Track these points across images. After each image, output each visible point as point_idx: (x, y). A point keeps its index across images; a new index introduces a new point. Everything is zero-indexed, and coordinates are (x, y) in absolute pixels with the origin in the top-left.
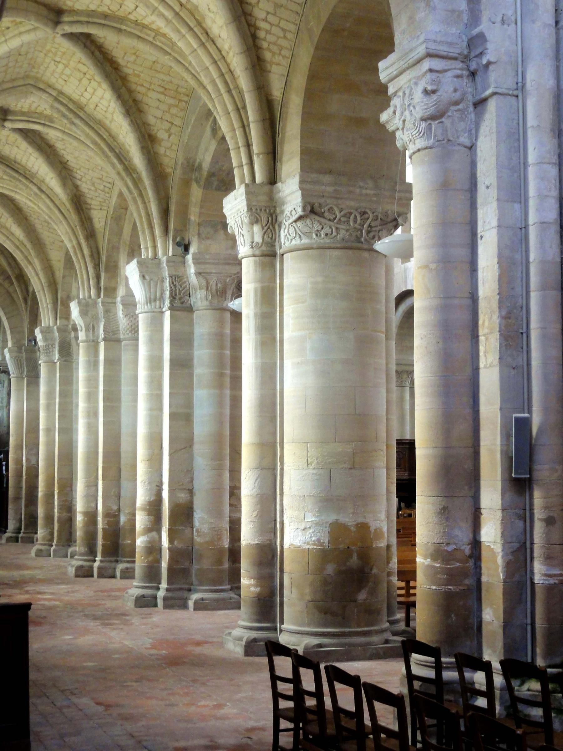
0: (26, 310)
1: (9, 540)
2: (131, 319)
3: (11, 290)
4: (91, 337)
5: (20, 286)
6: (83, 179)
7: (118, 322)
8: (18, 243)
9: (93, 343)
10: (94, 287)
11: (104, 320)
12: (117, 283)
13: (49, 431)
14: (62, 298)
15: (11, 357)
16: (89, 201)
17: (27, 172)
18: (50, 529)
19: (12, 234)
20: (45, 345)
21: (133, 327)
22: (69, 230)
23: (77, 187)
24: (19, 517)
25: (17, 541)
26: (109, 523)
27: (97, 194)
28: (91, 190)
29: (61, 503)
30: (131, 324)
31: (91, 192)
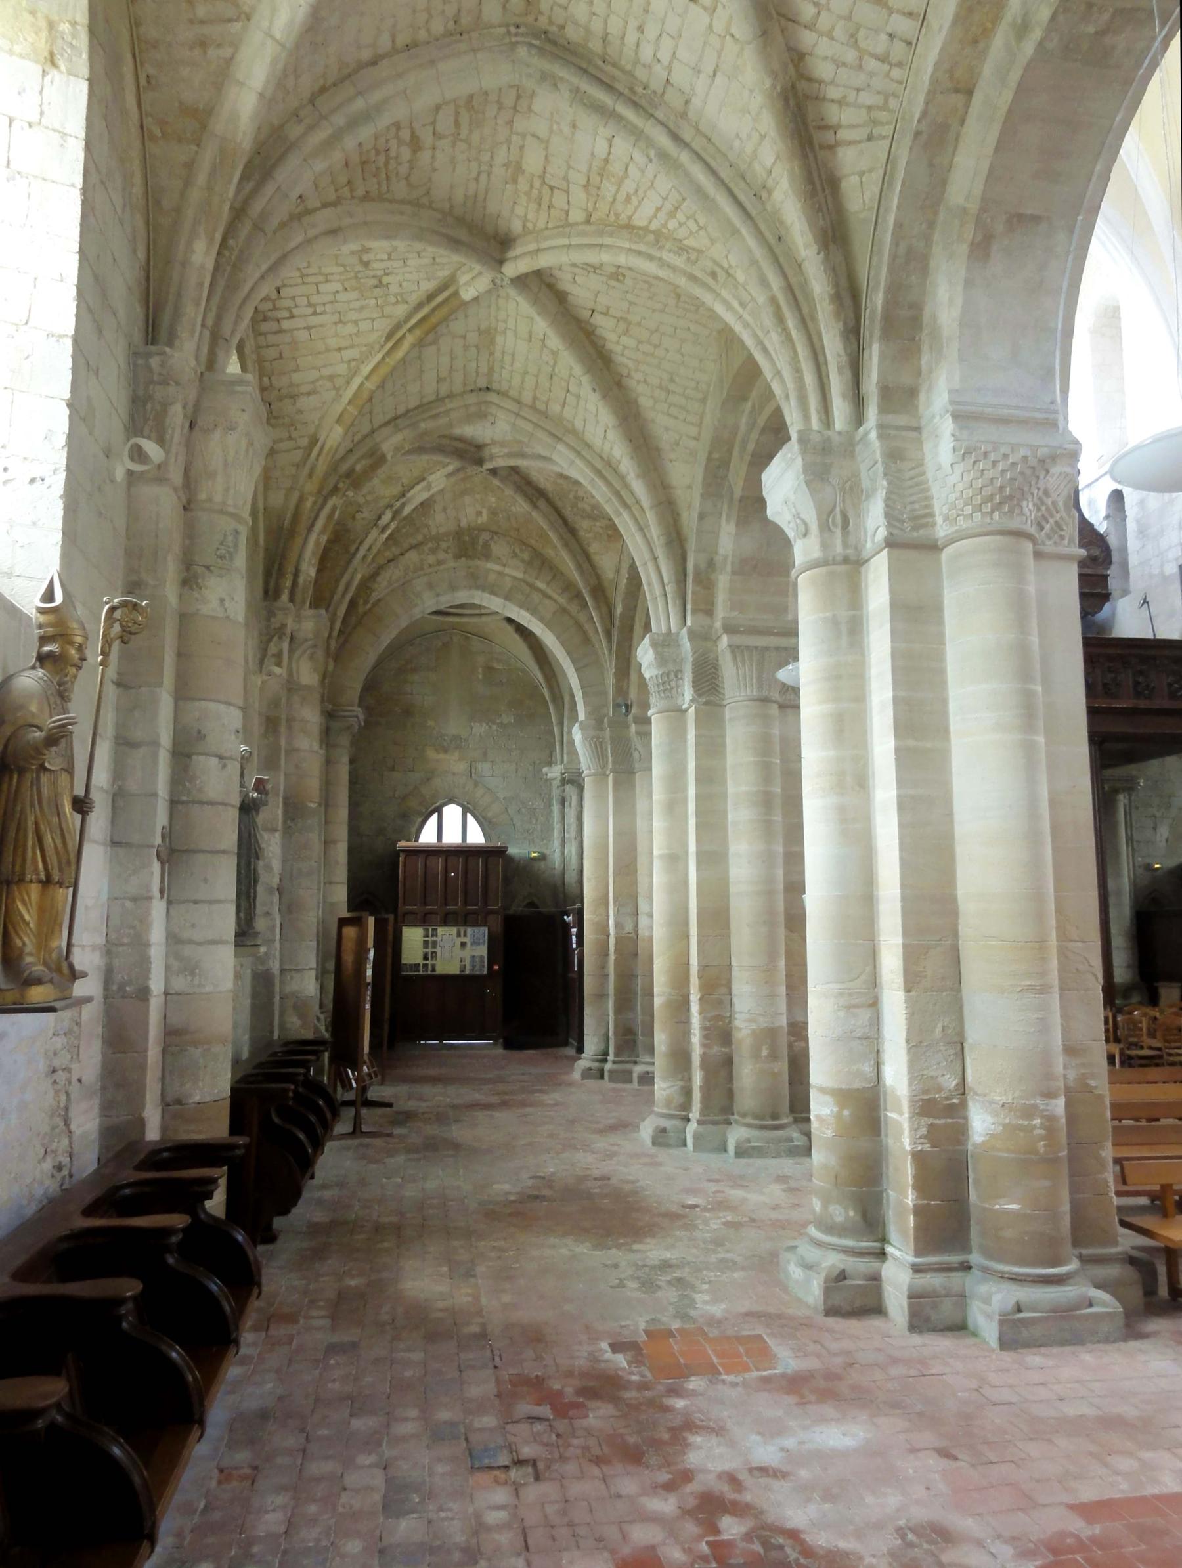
0: (610, 650)
1: (587, 1074)
2: (981, 465)
3: (582, 617)
4: (839, 549)
5: (598, 608)
6: (824, 22)
7: (928, 490)
8: (599, 465)
9: (844, 568)
10: (844, 396)
11: (885, 483)
12: (919, 373)
13: (675, 859)
14: (696, 567)
15: (585, 738)
16: (834, 114)
17: (639, 90)
18: (682, 1080)
19: (588, 446)
20: (661, 675)
21: (988, 491)
22: (759, 253)
23: (797, 58)
24: (603, 1031)
25: (602, 1077)
26: (932, 1134)
27: (860, 79)
28: (844, 64)
29: (708, 1024)
30: (980, 483)
31: (843, 74)
